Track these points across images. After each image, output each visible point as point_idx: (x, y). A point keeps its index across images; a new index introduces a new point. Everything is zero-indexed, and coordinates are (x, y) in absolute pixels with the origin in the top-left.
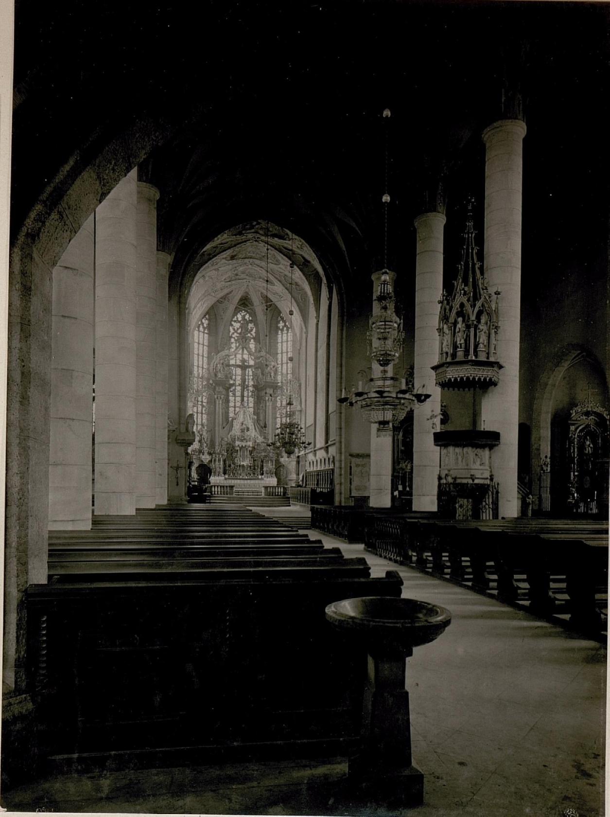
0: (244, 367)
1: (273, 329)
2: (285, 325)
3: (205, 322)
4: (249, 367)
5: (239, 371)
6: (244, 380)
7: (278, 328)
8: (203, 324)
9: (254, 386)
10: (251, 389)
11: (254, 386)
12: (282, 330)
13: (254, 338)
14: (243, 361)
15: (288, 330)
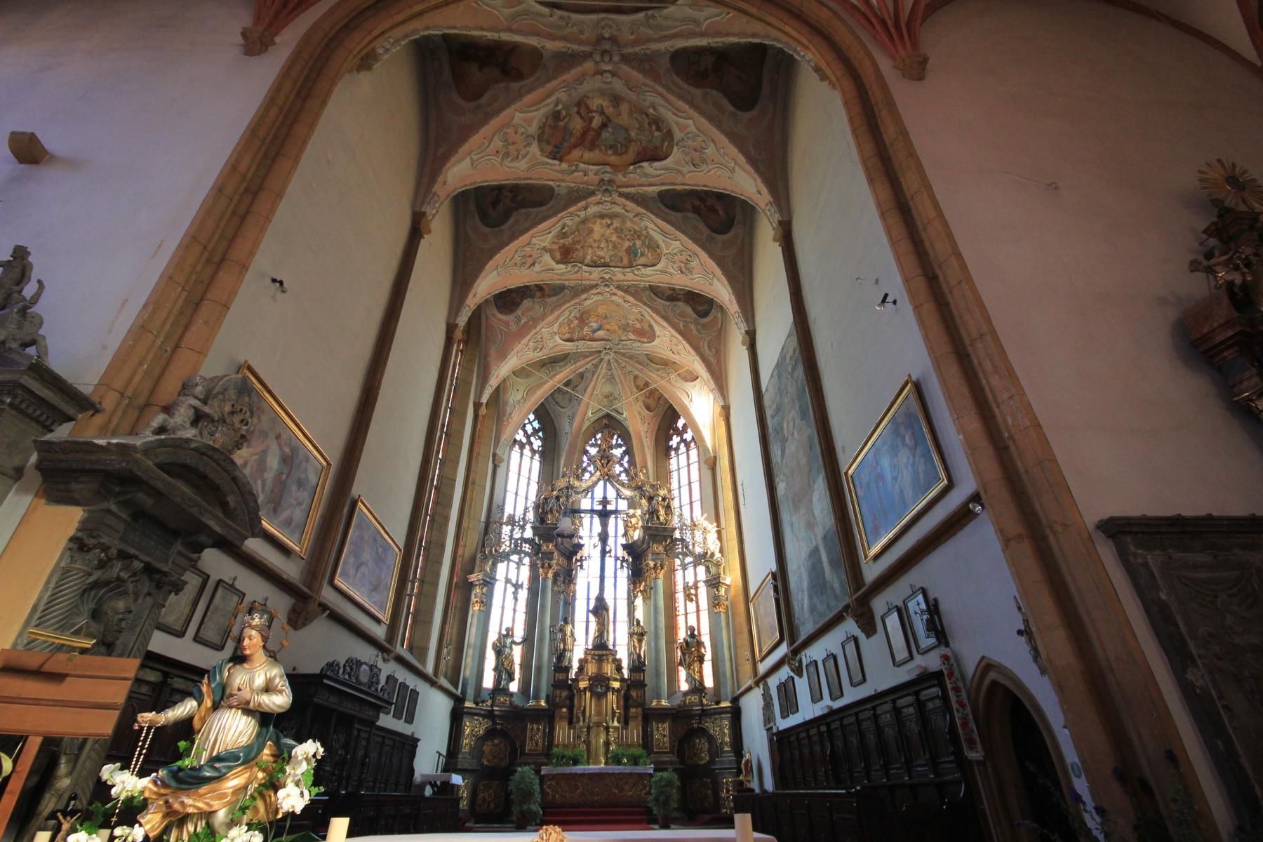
0: (604, 515)
1: (664, 452)
2: (684, 441)
3: (537, 444)
4: (616, 512)
5: (596, 520)
6: (604, 537)
7: (669, 448)
8: (531, 444)
9: (625, 547)
10: (621, 553)
11: (625, 547)
12: (677, 449)
13: (626, 471)
14: (605, 502)
15: (687, 445)
